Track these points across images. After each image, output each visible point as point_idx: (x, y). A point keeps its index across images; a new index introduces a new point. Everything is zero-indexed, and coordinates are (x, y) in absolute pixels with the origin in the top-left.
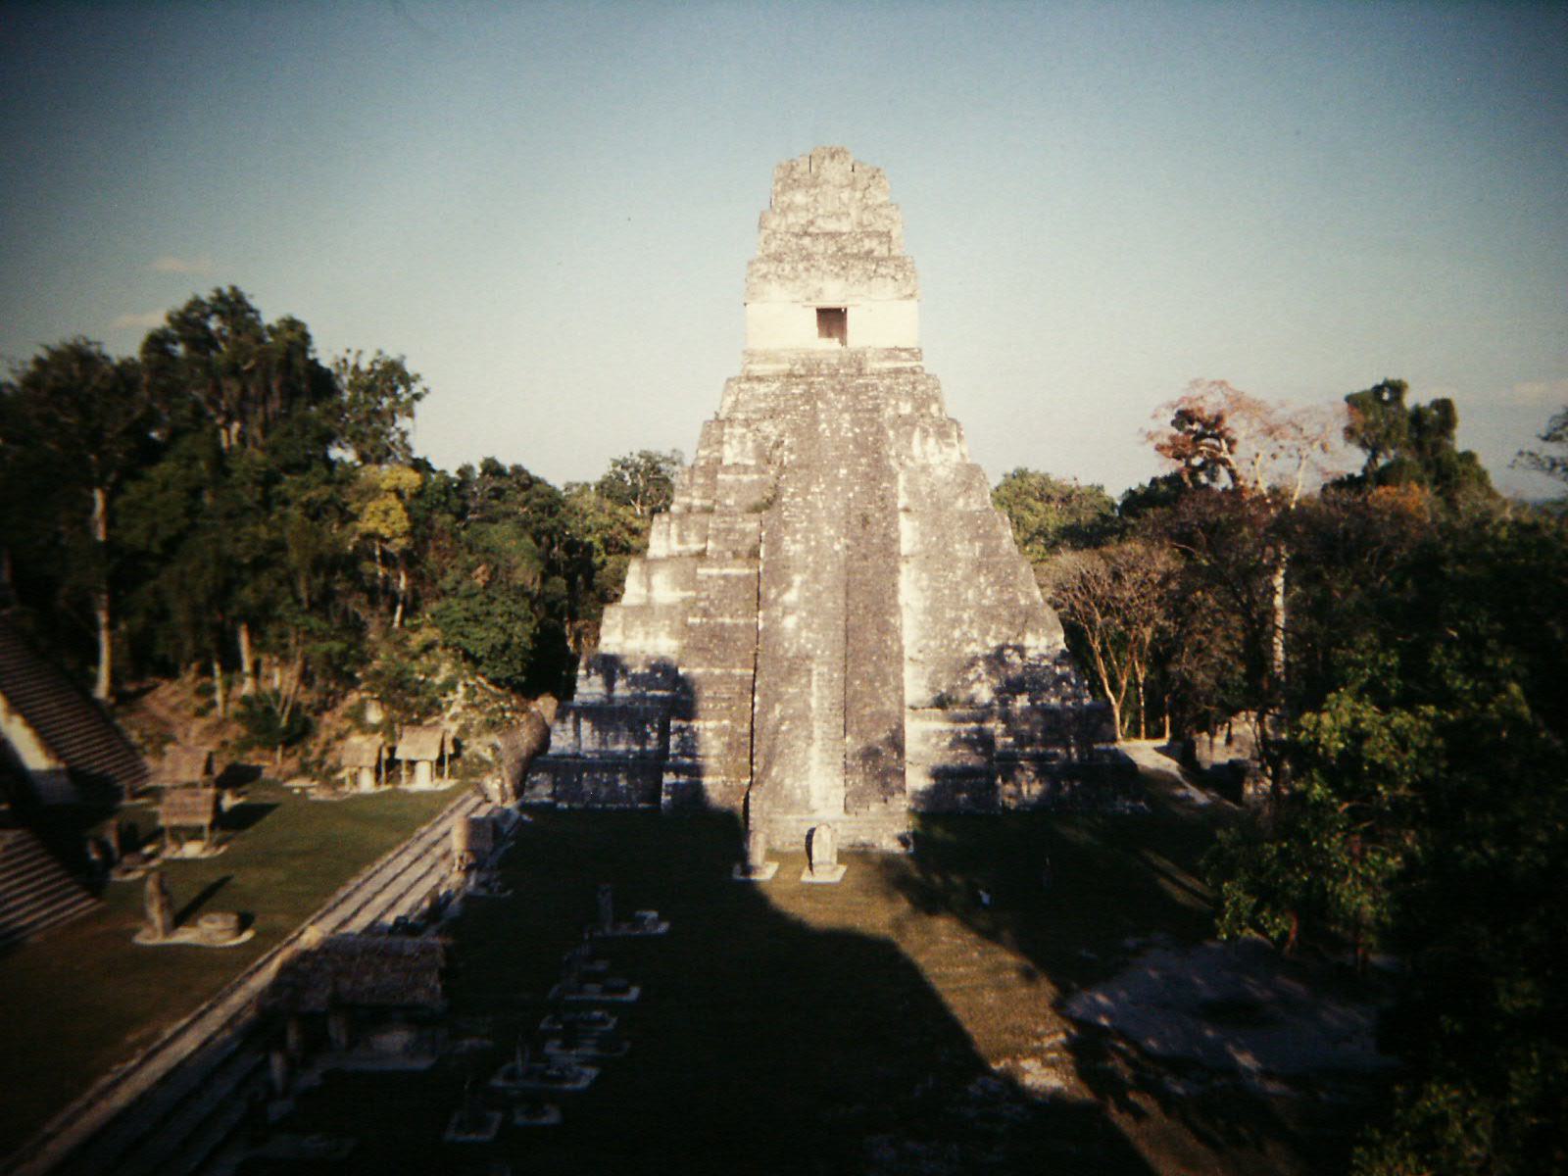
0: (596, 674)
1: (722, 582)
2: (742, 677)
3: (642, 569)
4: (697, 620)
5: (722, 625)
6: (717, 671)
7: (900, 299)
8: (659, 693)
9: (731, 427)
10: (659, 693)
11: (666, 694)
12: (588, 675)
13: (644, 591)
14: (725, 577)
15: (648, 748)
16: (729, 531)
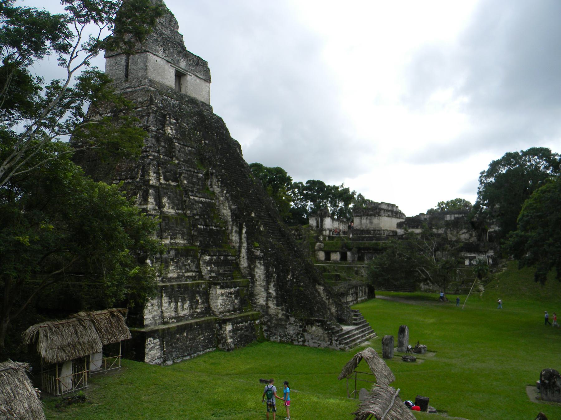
0: (156, 262)
1: (201, 205)
2: (232, 260)
3: (156, 192)
4: (202, 227)
5: (212, 229)
6: (222, 258)
7: (205, 80)
8: (190, 274)
9: (170, 118)
10: (190, 274)
11: (194, 274)
12: (152, 263)
13: (157, 208)
14: (201, 202)
15: (199, 311)
16: (192, 176)
